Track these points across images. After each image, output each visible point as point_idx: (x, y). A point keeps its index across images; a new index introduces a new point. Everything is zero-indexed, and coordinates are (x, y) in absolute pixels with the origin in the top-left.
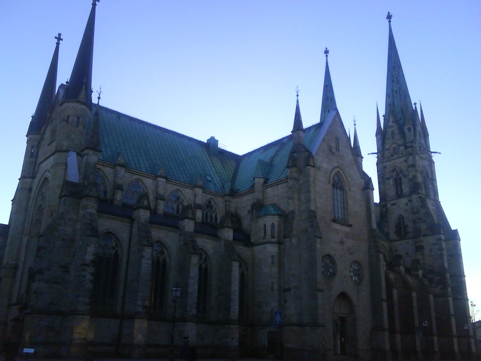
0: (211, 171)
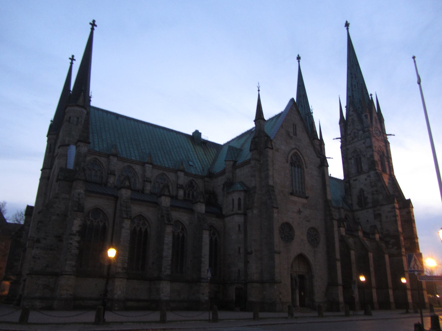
0: (193, 158)
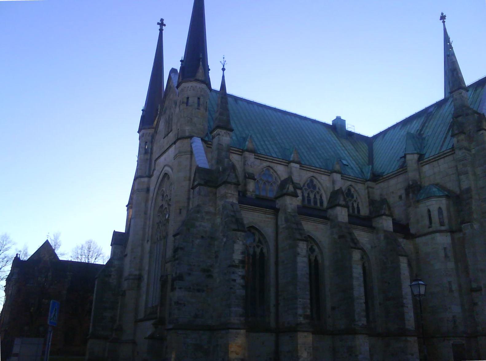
0: (344, 155)
